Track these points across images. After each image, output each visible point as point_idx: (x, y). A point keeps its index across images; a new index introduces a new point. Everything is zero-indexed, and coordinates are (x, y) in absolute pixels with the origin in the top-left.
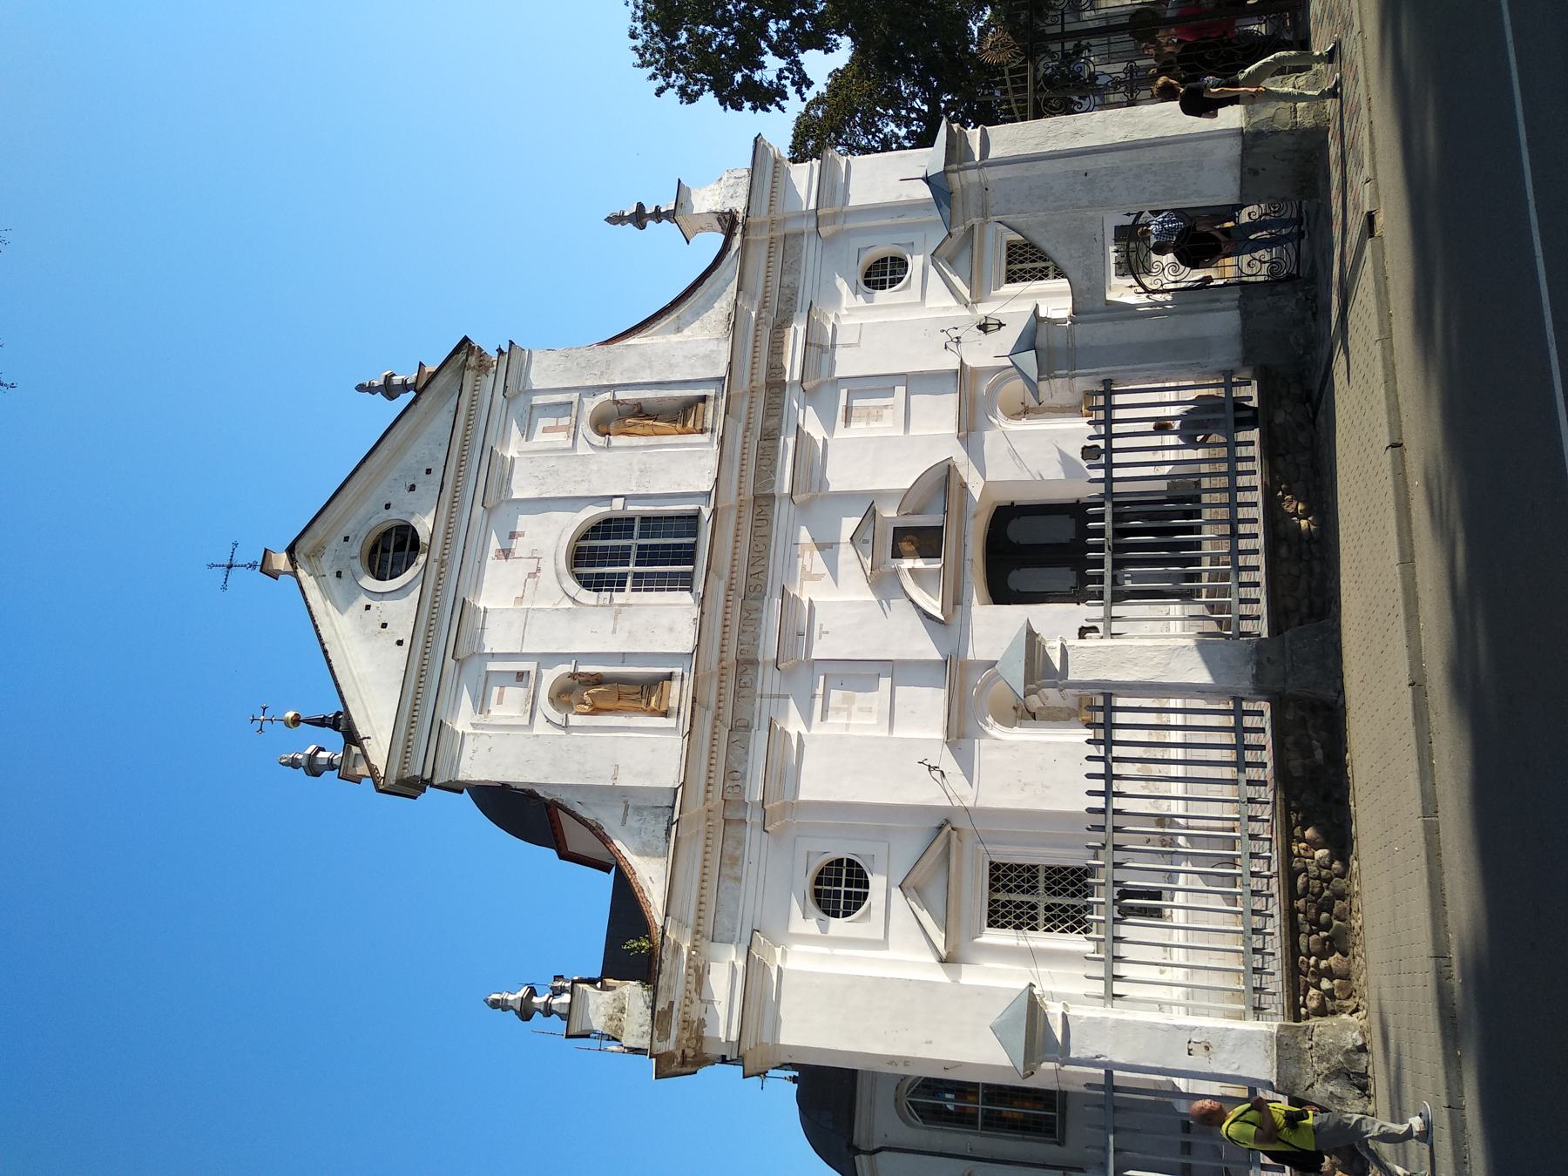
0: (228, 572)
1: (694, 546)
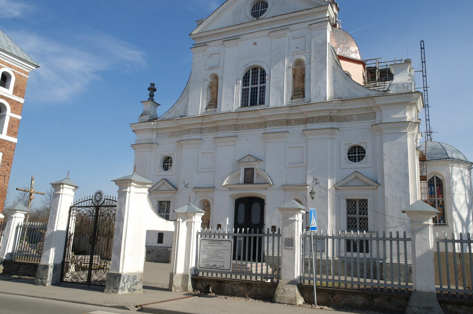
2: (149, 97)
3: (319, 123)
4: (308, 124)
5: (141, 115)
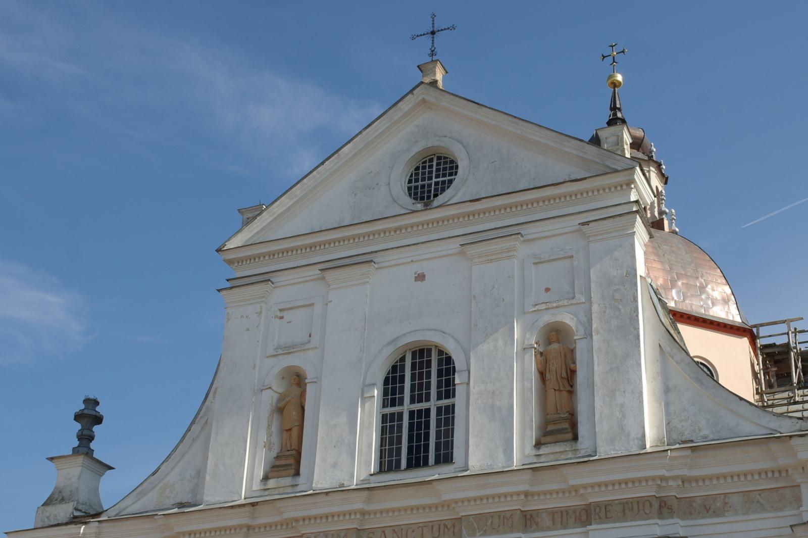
0: (427, 34)
2: (76, 443)
3: (626, 521)
4: (591, 525)
5: (48, 502)
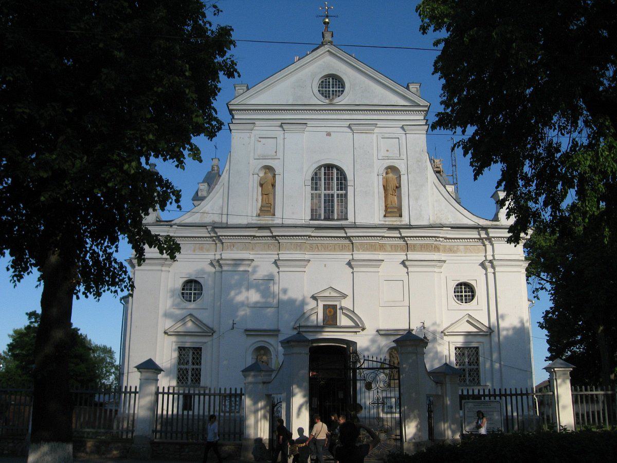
1: (333, 220)
